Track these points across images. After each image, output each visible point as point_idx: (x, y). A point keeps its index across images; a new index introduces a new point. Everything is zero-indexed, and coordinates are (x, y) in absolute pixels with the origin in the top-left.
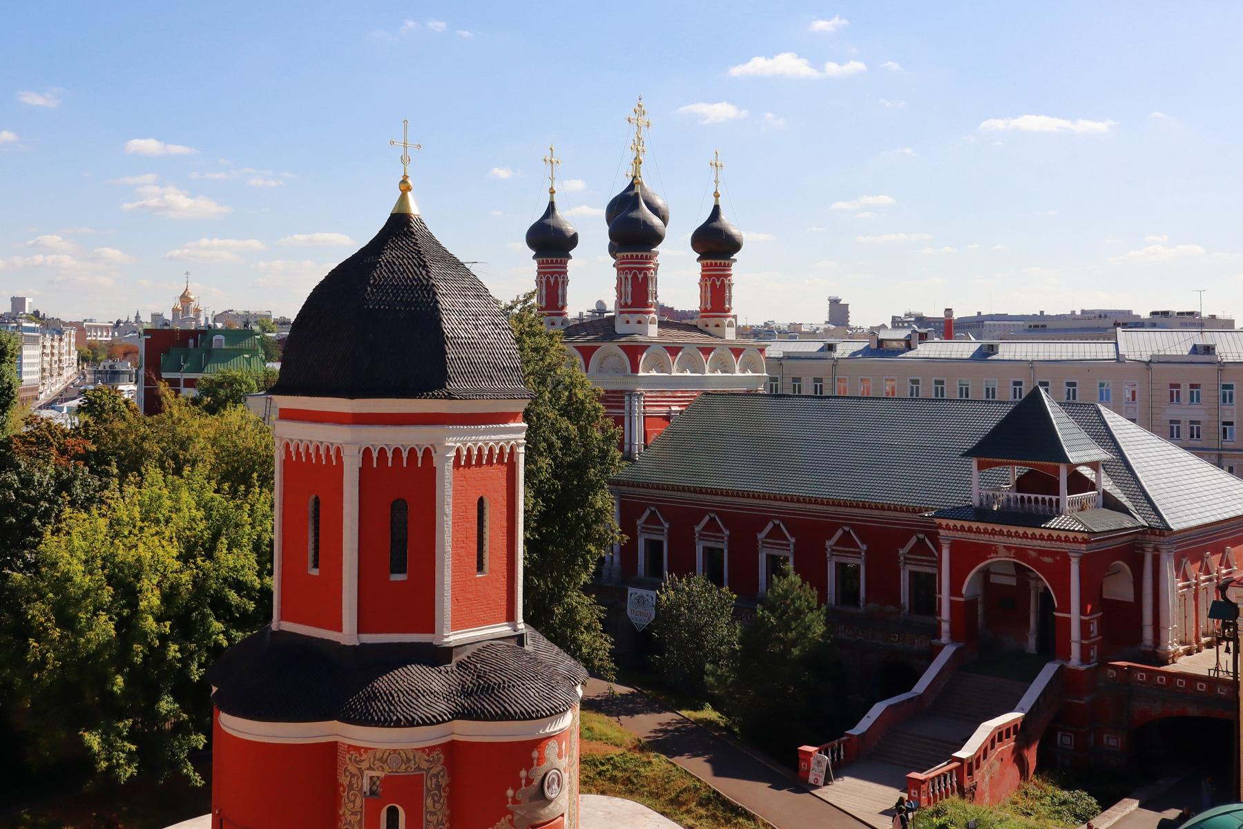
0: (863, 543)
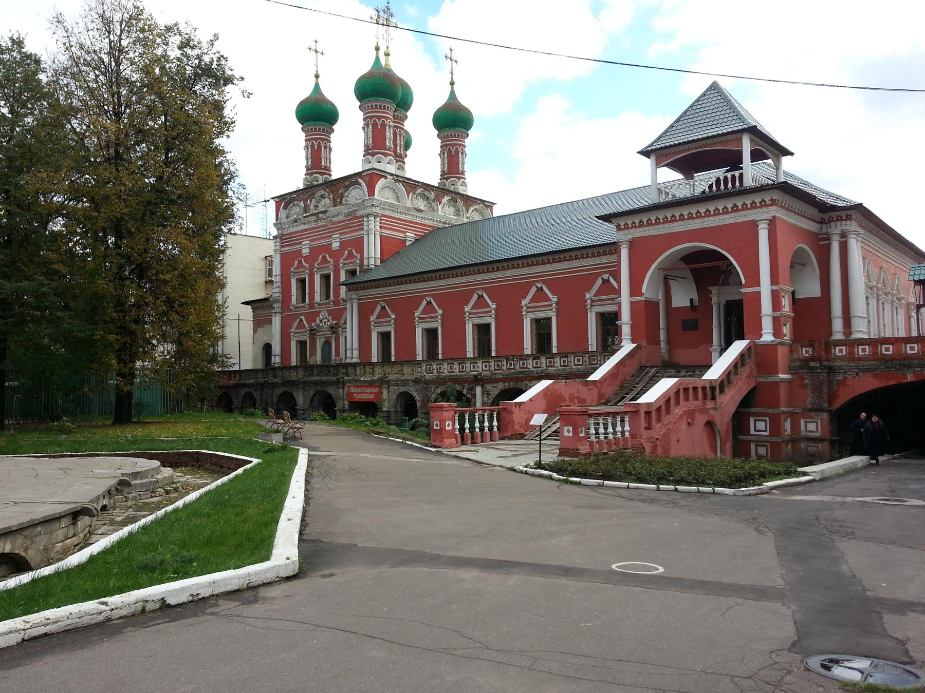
0: (554, 294)
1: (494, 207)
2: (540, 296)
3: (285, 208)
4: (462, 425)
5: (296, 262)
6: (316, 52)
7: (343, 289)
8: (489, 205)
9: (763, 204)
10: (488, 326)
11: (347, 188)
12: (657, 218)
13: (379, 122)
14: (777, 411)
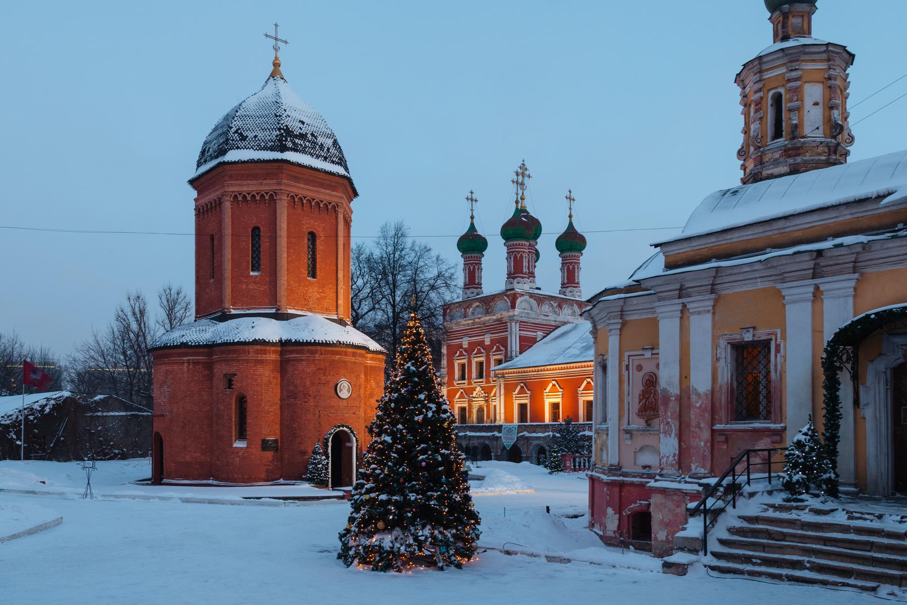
6: (472, 200)
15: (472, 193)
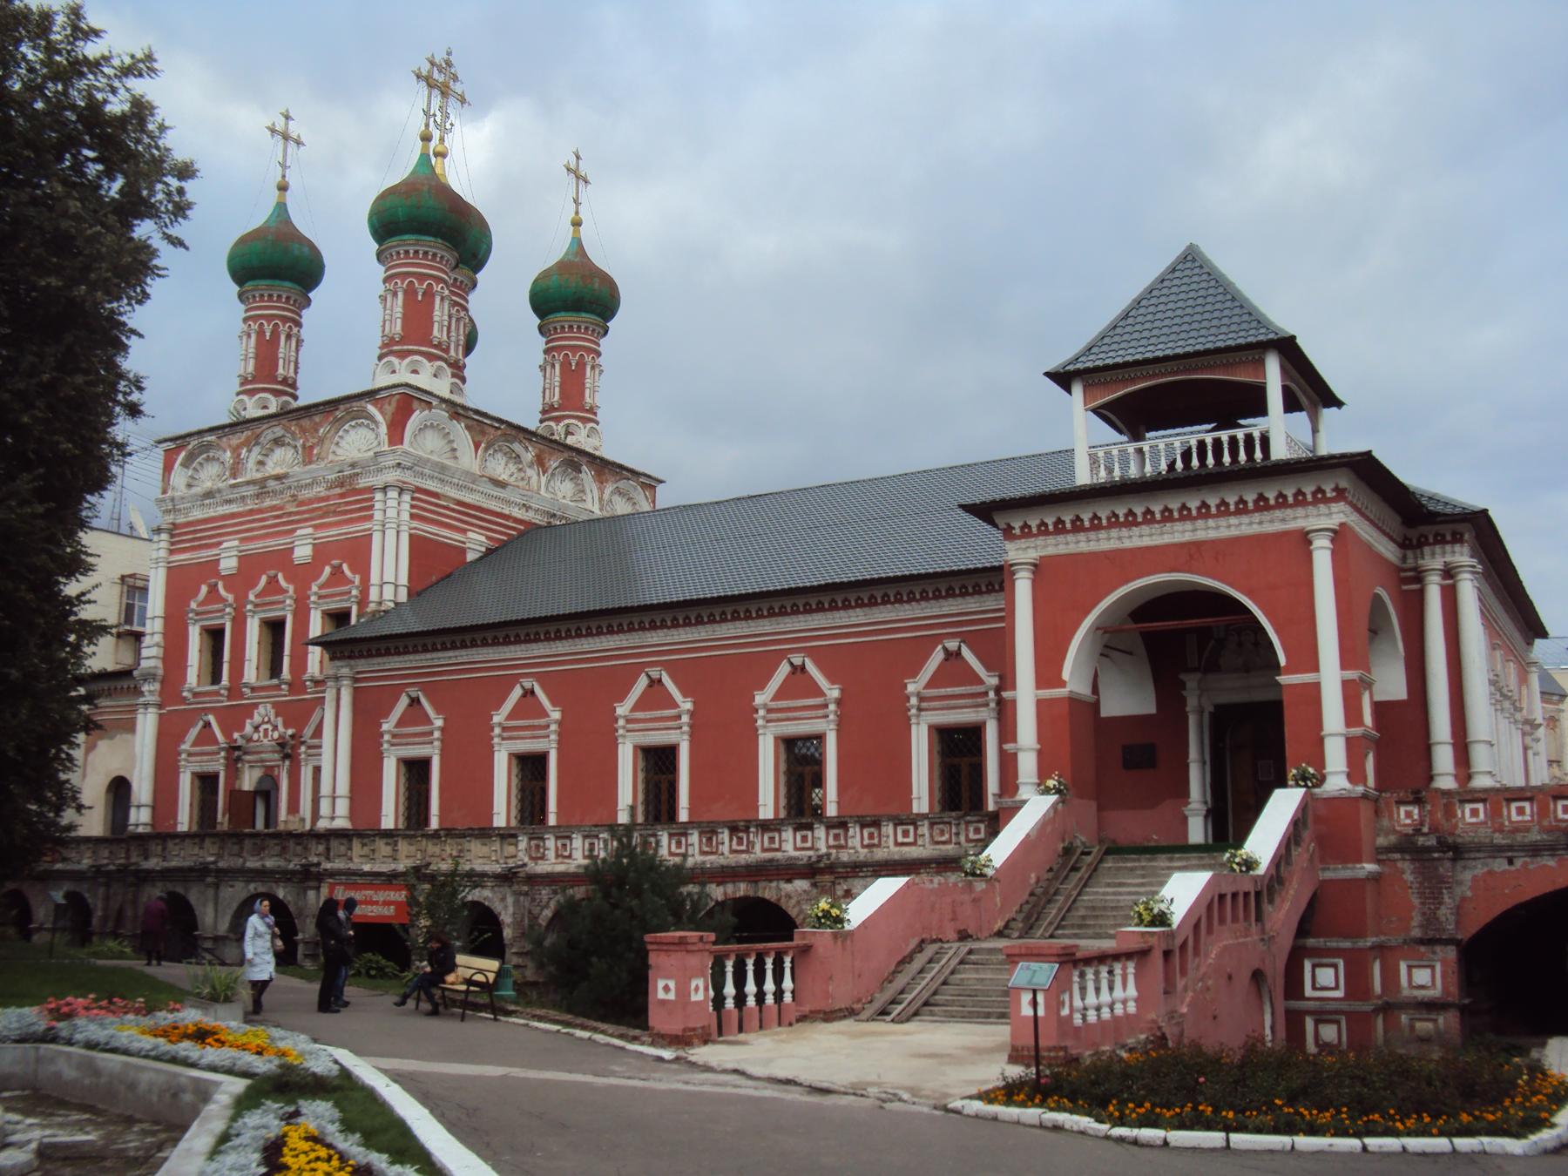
0: (832, 680)
1: (660, 488)
2: (799, 683)
3: (185, 465)
4: (718, 986)
5: (204, 589)
6: (286, 137)
7: (315, 653)
8: (649, 483)
9: (1320, 498)
10: (670, 752)
11: (339, 423)
12: (1095, 517)
13: (421, 288)
14: (1361, 944)
15: (287, 117)
